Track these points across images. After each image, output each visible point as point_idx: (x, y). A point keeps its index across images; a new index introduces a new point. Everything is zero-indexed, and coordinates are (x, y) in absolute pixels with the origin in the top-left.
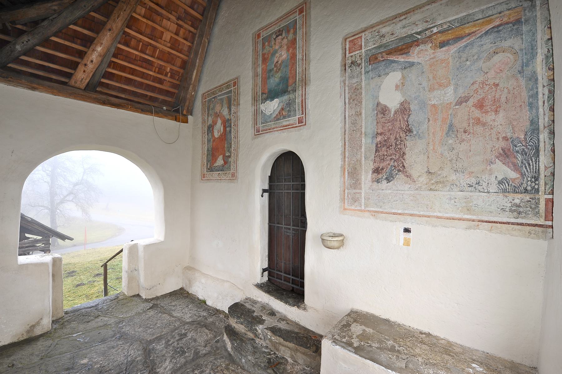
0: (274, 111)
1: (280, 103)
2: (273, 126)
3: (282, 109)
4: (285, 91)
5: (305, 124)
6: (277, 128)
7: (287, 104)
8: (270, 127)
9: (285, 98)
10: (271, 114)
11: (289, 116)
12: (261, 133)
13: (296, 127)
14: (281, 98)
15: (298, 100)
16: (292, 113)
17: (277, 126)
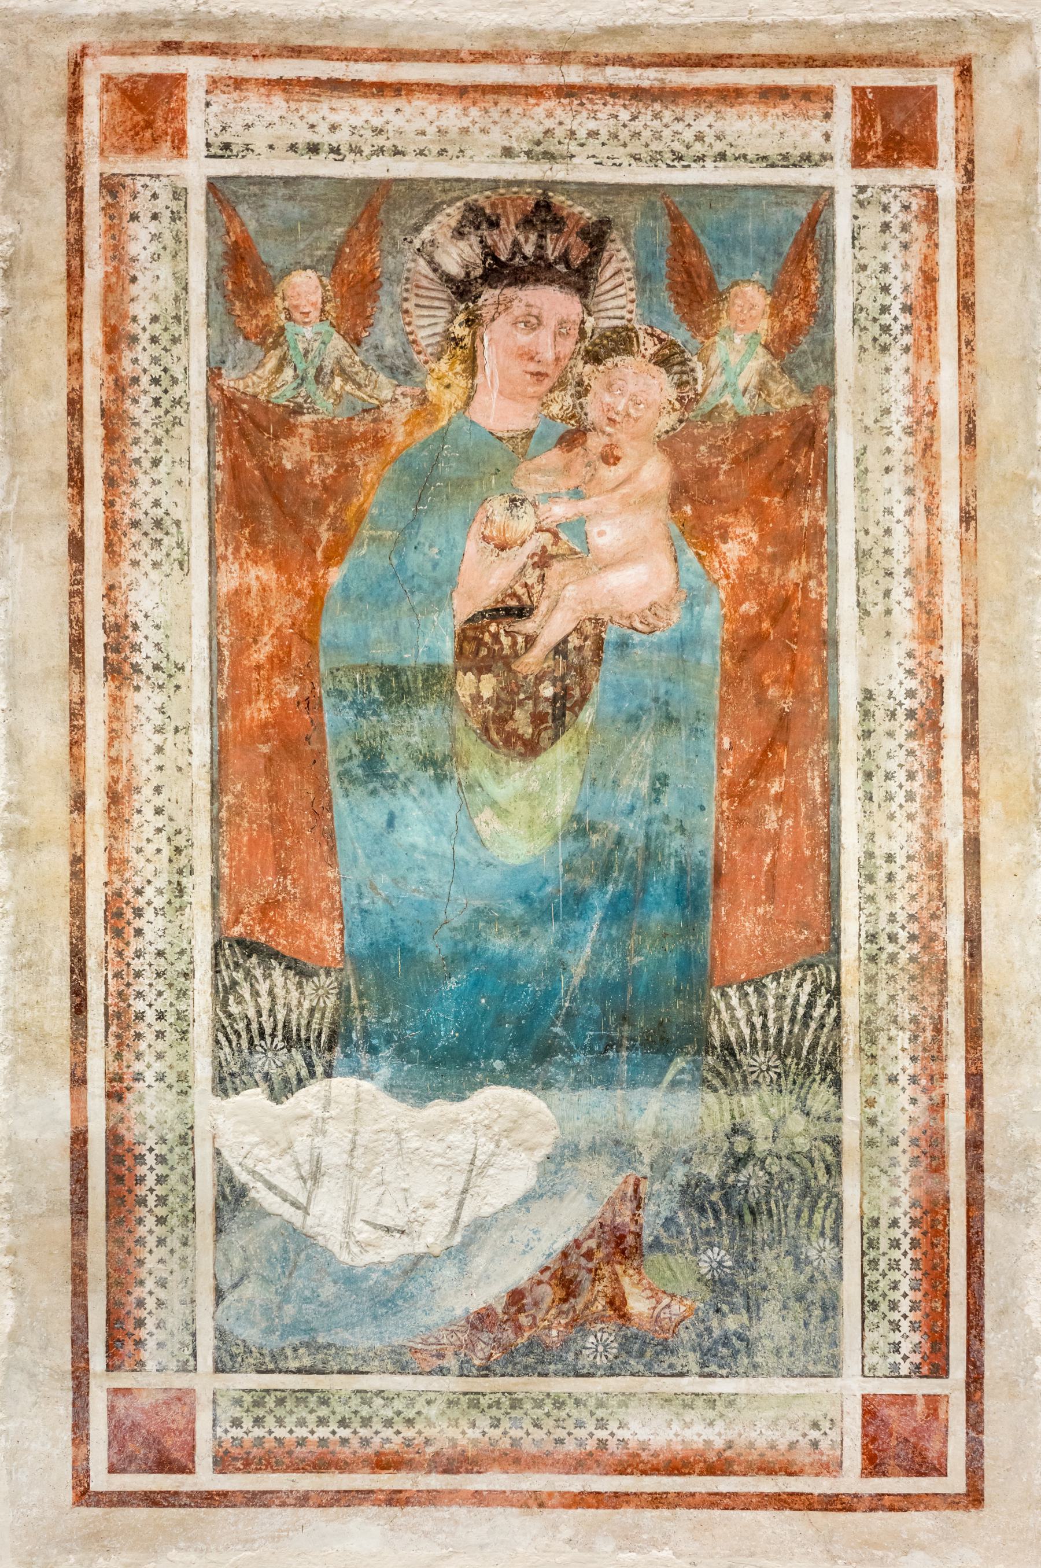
0: (469, 1239)
1: (562, 1158)
2: (447, 1432)
3: (621, 1245)
4: (650, 1026)
5: (974, 1496)
6: (514, 1460)
7: (694, 1196)
8: (389, 1439)
9: (671, 1114)
10: (414, 1266)
11: (722, 1354)
12: (205, 1477)
13: (833, 1503)
14: (594, 1109)
15: (875, 1193)
16: (774, 1325)
17: (533, 1440)
